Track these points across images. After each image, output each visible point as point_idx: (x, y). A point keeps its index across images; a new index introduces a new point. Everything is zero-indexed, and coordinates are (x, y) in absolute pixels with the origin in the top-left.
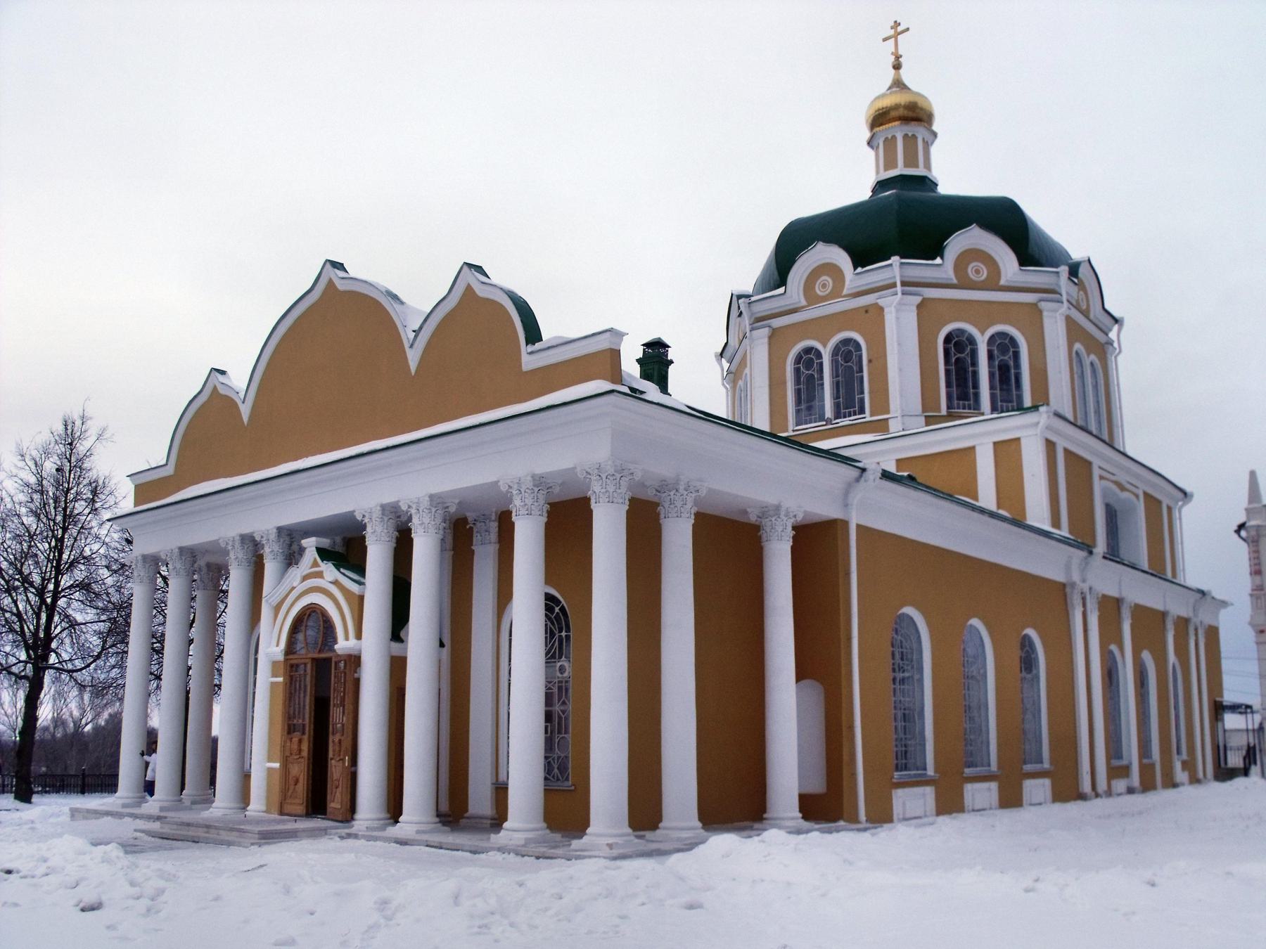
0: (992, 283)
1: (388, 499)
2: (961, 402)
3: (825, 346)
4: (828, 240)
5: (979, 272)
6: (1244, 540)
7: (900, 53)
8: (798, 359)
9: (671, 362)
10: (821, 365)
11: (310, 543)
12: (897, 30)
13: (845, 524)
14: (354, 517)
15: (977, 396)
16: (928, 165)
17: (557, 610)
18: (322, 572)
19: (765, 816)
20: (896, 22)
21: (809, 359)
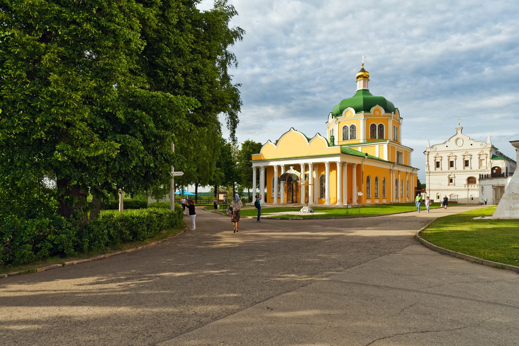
0: (379, 115)
5: (377, 113)
13: (362, 164)
16: (367, 87)
21: (345, 127)
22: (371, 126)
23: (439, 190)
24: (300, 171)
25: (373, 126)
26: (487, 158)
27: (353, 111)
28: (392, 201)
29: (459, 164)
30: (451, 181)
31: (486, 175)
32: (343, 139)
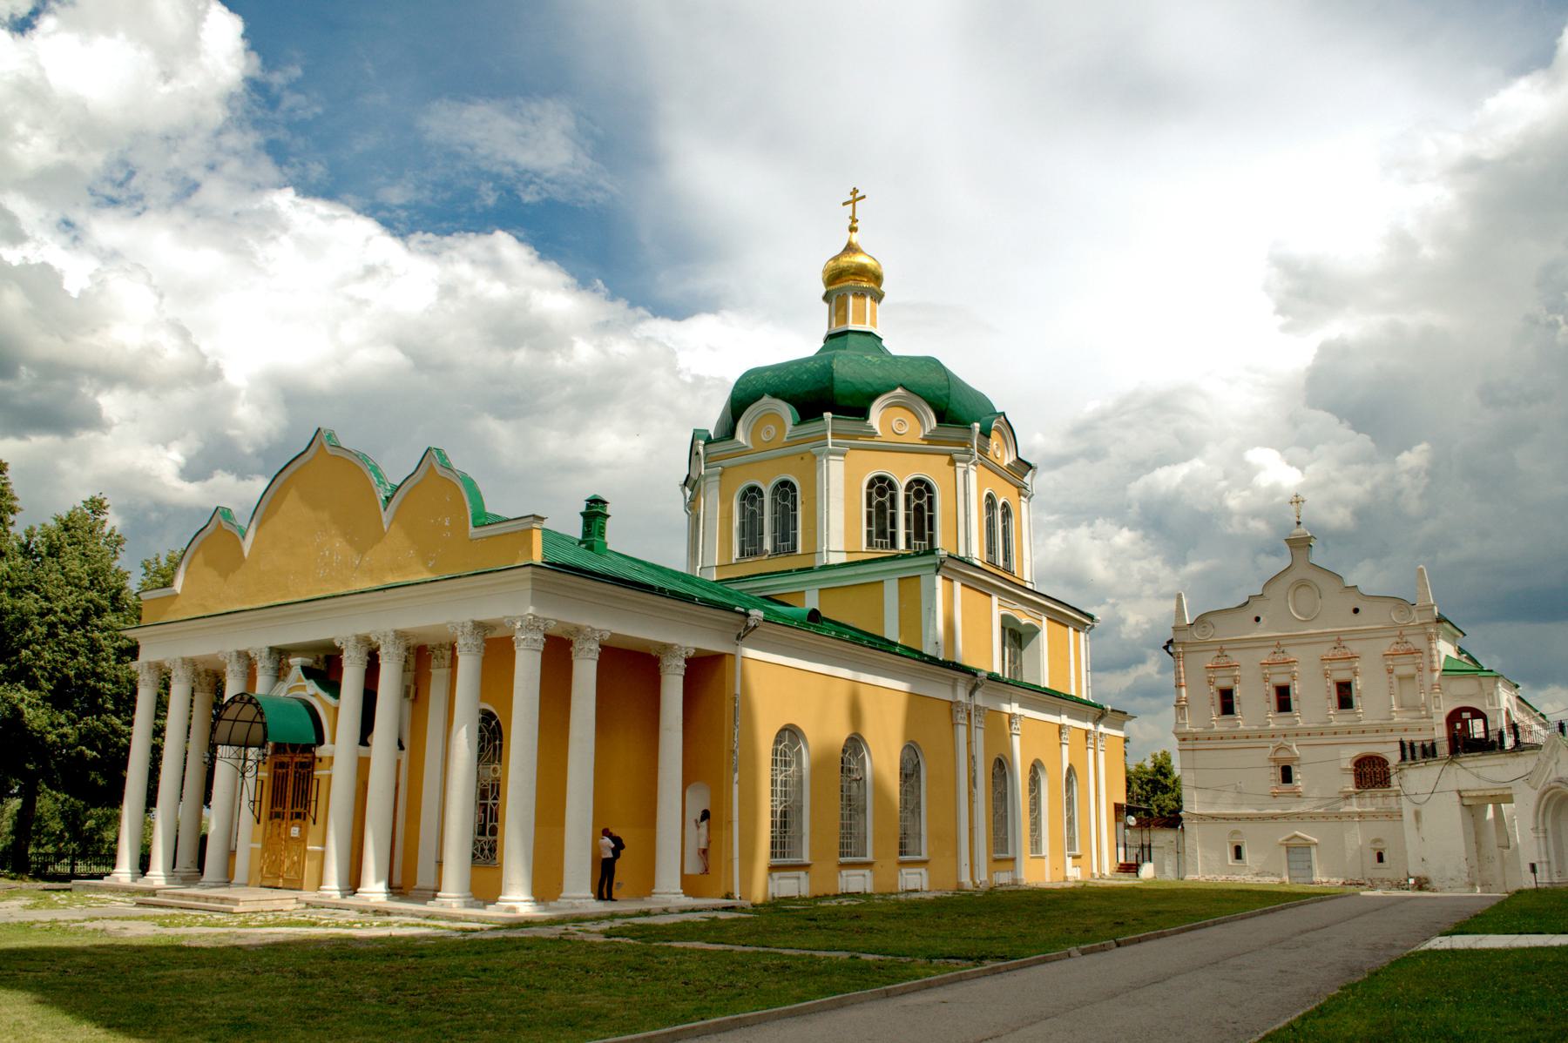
1: (362, 631)
2: (879, 540)
3: (766, 485)
4: (775, 395)
6: (1171, 654)
7: (857, 218)
8: (744, 497)
9: (608, 516)
10: (763, 501)
11: (296, 662)
12: (855, 197)
14: (334, 643)
15: (893, 536)
16: (873, 323)
17: (493, 723)
18: (305, 686)
19: (654, 891)
20: (855, 191)
21: (752, 495)
22: (871, 485)
23: (1237, 818)
24: (332, 686)
25: (881, 486)
26: (1420, 670)
27: (787, 412)
28: (965, 879)
29: (1313, 701)
30: (1287, 775)
31: (1428, 745)
32: (742, 554)
